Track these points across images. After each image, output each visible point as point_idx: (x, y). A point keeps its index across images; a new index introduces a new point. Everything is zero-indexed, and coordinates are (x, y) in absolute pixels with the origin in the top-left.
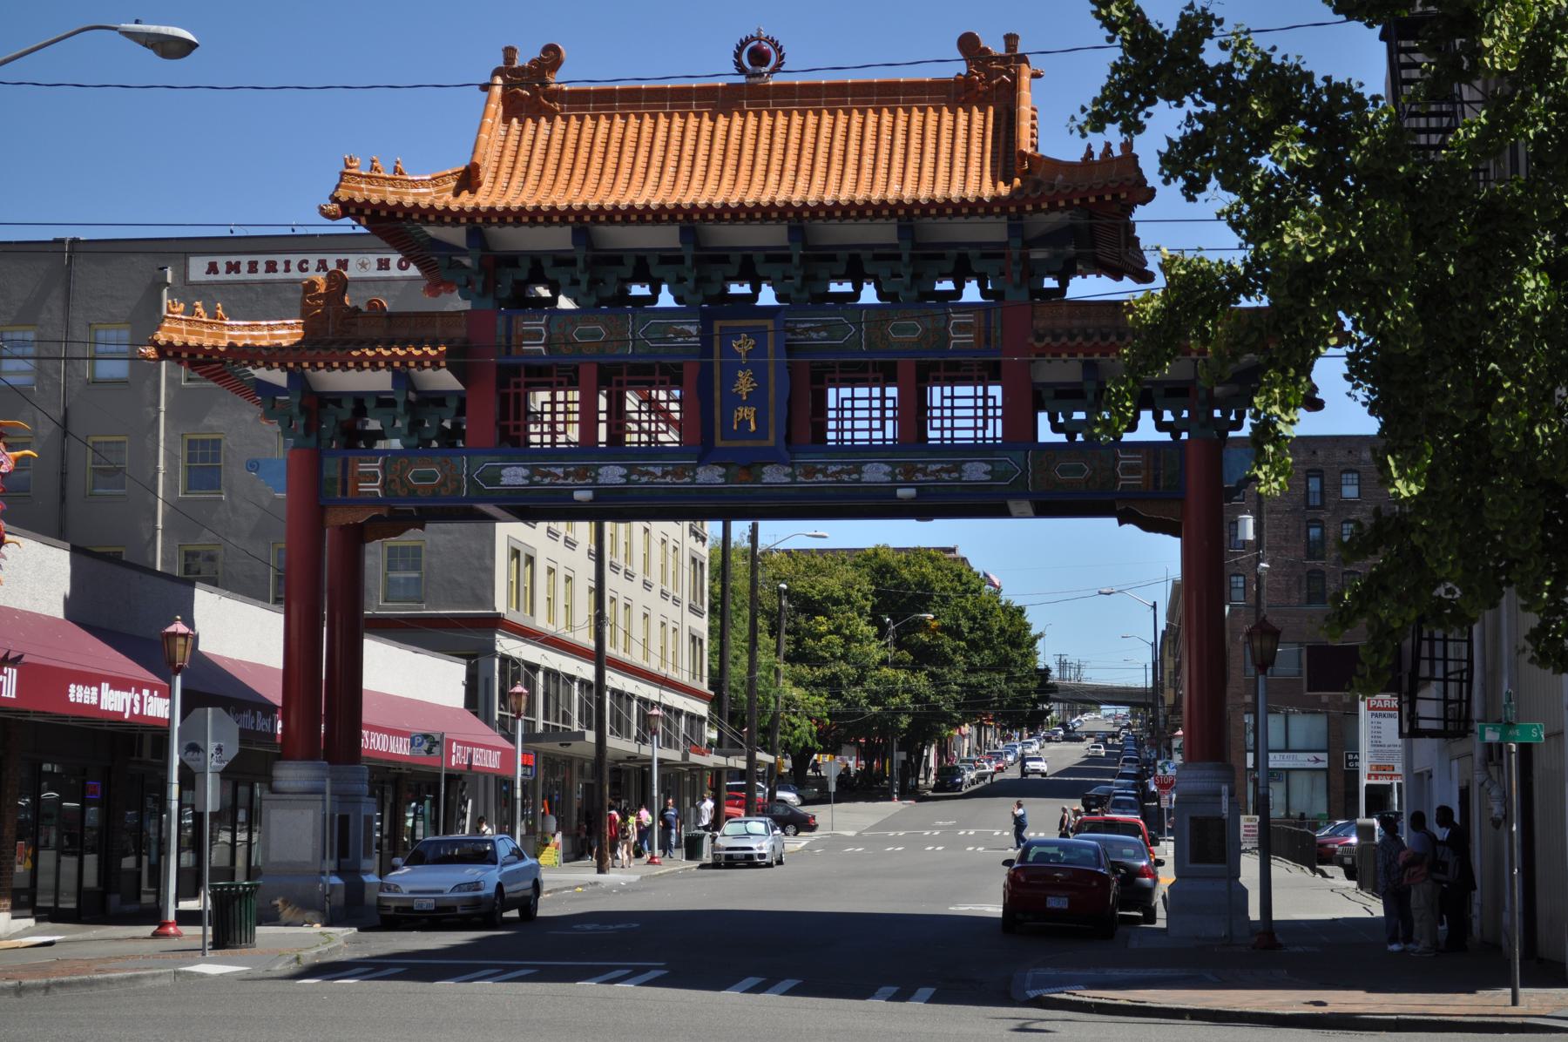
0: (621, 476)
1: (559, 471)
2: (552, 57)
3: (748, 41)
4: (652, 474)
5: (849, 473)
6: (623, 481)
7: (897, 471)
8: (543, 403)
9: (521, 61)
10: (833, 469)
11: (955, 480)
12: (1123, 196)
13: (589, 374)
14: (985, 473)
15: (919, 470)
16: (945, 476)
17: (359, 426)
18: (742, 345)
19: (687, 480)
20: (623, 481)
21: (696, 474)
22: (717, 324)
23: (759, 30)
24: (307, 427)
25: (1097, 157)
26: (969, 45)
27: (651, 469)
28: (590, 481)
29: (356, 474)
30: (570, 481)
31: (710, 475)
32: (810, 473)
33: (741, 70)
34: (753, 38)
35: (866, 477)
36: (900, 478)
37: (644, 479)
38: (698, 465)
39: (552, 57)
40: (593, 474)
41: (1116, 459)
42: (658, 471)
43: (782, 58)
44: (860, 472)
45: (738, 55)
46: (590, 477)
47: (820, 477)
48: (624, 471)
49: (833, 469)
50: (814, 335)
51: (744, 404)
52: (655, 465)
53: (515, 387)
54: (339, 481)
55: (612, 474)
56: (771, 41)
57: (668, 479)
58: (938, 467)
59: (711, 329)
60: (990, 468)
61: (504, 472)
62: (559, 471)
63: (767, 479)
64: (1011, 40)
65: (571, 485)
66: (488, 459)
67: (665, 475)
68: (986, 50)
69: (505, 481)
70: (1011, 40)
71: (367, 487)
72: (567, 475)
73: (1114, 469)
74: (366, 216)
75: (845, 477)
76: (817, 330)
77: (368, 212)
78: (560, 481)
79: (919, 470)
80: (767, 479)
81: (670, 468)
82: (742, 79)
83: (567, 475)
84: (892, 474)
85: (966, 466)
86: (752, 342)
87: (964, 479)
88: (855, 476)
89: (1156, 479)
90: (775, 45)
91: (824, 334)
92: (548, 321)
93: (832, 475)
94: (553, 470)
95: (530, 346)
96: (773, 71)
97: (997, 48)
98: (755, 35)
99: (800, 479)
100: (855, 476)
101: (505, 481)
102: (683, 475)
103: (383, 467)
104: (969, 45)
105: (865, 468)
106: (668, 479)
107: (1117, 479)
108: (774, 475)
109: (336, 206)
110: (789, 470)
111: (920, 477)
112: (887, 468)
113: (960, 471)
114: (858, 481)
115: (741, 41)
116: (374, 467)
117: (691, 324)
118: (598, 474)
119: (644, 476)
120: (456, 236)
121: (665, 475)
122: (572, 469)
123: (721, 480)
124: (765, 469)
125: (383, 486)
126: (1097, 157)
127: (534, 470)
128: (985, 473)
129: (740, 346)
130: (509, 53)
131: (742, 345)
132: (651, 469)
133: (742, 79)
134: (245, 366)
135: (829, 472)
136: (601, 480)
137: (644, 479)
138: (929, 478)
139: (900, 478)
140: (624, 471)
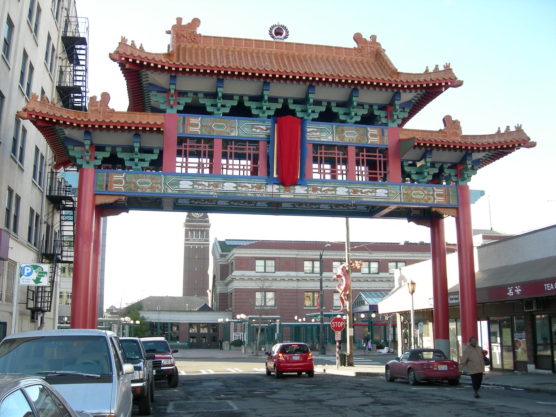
0: (233, 187)
1: (206, 184)
2: (196, 22)
4: (247, 187)
5: (331, 191)
6: (235, 189)
7: (350, 191)
9: (184, 23)
10: (324, 189)
14: (386, 194)
16: (370, 194)
19: (263, 190)
20: (235, 189)
21: (266, 188)
23: (278, 22)
26: (358, 38)
28: (220, 188)
30: (211, 188)
32: (315, 190)
33: (273, 37)
35: (338, 193)
36: (351, 194)
38: (267, 184)
39: (196, 22)
40: (221, 186)
43: (288, 32)
46: (220, 187)
47: (319, 192)
48: (235, 185)
49: (324, 189)
53: (185, 147)
58: (367, 190)
60: (387, 192)
61: (181, 182)
62: (206, 184)
63: (297, 191)
65: (211, 190)
66: (173, 177)
67: (253, 187)
68: (365, 39)
69: (181, 186)
71: (116, 187)
72: (209, 186)
76: (316, 132)
77: (130, 60)
78: (206, 188)
80: (297, 191)
81: (255, 185)
82: (272, 39)
83: (209, 186)
84: (348, 192)
85: (377, 191)
87: (377, 196)
91: (318, 134)
92: (201, 122)
93: (324, 191)
94: (203, 183)
95: (192, 129)
96: (285, 38)
98: (277, 25)
100: (333, 192)
101: (181, 186)
102: (260, 188)
103: (125, 178)
104: (358, 38)
105: (337, 189)
106: (254, 189)
107: (434, 199)
110: (306, 188)
111: (360, 194)
112: (347, 190)
113: (376, 193)
115: (272, 26)
117: (263, 125)
118: (223, 186)
119: (242, 187)
120: (161, 80)
121: (253, 187)
122: (212, 183)
123: (278, 191)
125: (124, 187)
127: (195, 183)
128: (386, 194)
130: (179, 20)
132: (247, 185)
133: (272, 39)
135: (323, 190)
136: (225, 189)
137: (244, 189)
138: (364, 195)
139: (351, 194)
140: (235, 185)
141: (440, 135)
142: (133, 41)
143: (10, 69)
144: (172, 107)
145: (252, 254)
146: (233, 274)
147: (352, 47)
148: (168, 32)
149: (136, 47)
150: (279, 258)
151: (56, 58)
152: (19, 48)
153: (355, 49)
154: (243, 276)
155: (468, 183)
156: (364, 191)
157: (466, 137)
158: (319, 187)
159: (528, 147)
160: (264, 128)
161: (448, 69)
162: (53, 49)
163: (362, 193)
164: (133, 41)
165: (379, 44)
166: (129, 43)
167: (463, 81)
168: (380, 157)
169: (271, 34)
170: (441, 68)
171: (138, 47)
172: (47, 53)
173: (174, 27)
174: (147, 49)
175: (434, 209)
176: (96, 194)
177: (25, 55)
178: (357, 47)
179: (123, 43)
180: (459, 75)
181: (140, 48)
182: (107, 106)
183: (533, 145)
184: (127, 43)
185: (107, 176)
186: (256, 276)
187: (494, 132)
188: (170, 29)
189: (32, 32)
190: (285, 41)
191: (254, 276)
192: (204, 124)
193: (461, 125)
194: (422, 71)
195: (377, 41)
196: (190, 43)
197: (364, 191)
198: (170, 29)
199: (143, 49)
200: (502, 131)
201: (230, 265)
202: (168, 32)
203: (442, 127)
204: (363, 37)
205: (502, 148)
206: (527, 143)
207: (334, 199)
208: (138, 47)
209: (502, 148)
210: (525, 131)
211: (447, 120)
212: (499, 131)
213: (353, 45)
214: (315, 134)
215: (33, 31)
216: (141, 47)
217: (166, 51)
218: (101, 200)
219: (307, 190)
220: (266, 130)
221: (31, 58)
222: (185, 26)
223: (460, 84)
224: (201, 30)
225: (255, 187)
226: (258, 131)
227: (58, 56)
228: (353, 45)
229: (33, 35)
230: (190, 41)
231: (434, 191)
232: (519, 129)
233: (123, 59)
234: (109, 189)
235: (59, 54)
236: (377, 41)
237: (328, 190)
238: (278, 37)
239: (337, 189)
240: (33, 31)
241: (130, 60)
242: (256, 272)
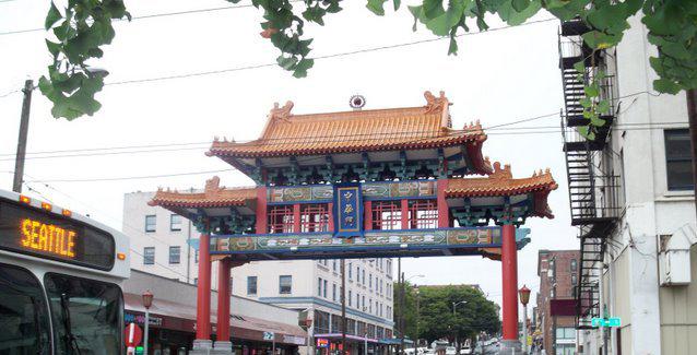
13: (297, 209)
18: (348, 195)
31: (337, 242)
108: (359, 241)
131: (348, 195)
179: (216, 142)
232: (548, 171)
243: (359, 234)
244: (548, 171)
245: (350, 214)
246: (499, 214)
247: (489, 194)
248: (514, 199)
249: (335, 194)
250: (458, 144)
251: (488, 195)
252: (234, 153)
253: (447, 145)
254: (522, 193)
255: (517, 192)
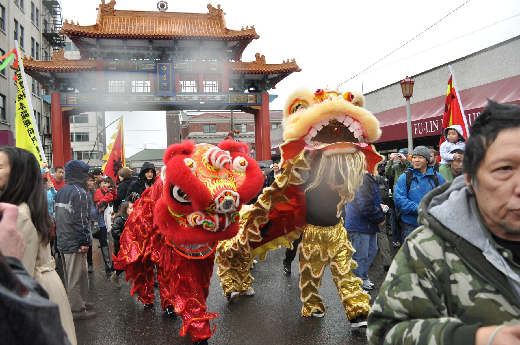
3: (158, 3)
4: (144, 98)
5: (189, 98)
8: (112, 84)
10: (185, 98)
11: (213, 100)
12: (252, 37)
15: (205, 98)
16: (211, 99)
17: (67, 89)
21: (154, 98)
22: (158, 64)
24: (56, 86)
25: (245, 29)
26: (209, 6)
27: (143, 97)
29: (70, 99)
31: (158, 99)
33: (159, 9)
34: (161, 2)
35: (193, 100)
36: (201, 100)
37: (142, 100)
39: (113, 3)
41: (248, 96)
42: (145, 98)
44: (192, 98)
45: (157, 6)
47: (183, 100)
48: (137, 98)
49: (185, 98)
50: (180, 67)
51: (165, 82)
52: (144, 96)
54: (65, 100)
55: (134, 99)
56: (165, 2)
57: (147, 100)
58: (209, 97)
59: (157, 65)
64: (219, 6)
67: (147, 98)
70: (219, 6)
73: (247, 99)
74: (71, 34)
75: (189, 99)
76: (181, 66)
77: (71, 33)
79: (205, 98)
82: (159, 11)
85: (216, 97)
86: (166, 68)
88: (191, 99)
89: (256, 101)
90: (166, 3)
92: (116, 63)
96: (166, 9)
97: (216, 7)
99: (178, 100)
100: (191, 99)
103: (76, 97)
104: (209, 6)
105: (193, 97)
106: (147, 100)
107: (248, 100)
108: (172, 99)
109: (63, 31)
110: (176, 98)
111: (205, 99)
113: (214, 98)
114: (191, 100)
116: (74, 96)
119: (141, 99)
124: (170, 97)
126: (245, 29)
129: (163, 69)
132: (143, 97)
133: (159, 11)
134: (40, 71)
137: (142, 100)
139: (201, 100)
140: (137, 98)
141: (252, 64)
142: (72, 21)
143: (6, 35)
144: (99, 56)
145: (201, 121)
146: (190, 134)
147: (206, 13)
148: (97, 9)
149: (74, 24)
150: (218, 123)
151: (40, 15)
152: (10, 21)
153: (208, 14)
154: (195, 135)
155: (268, 91)
156: (208, 98)
157: (268, 65)
158: (183, 97)
159: (298, 71)
160: (151, 65)
161: (253, 29)
162: (37, 10)
163: (207, 99)
164: (72, 21)
165: (222, 10)
166: (70, 22)
167: (259, 36)
168: (218, 78)
169: (158, 7)
170: (250, 28)
171: (76, 24)
172: (32, 14)
173: (100, 5)
174: (81, 25)
175: (248, 106)
176: (61, 106)
177: (16, 22)
178: (209, 12)
180: (258, 32)
181: (77, 24)
182: (63, 57)
183: (300, 70)
184: (69, 23)
185: (67, 95)
186: (204, 136)
187: (281, 62)
188: (98, 7)
189: (18, 7)
190: (166, 11)
191: (203, 136)
192: (118, 65)
193: (266, 58)
194: (240, 29)
195: (221, 8)
196: (110, 15)
197: (208, 98)
198: (98, 7)
199: (79, 25)
200: (285, 62)
201: (188, 128)
202: (97, 9)
203: (254, 59)
204: (213, 6)
205: (286, 71)
206: (297, 69)
207: (192, 103)
208: (76, 24)
209: (286, 71)
210: (297, 63)
211: (257, 55)
212: (284, 62)
213: (207, 11)
214: (180, 67)
215: (20, 6)
216: (78, 24)
217: (94, 23)
218: (64, 109)
219: (176, 99)
220: (153, 67)
221: (20, 22)
222: (107, 5)
223: (258, 37)
224: (116, 7)
225: (147, 98)
226: (148, 67)
227: (41, 14)
228: (207, 11)
229: (20, 9)
230: (110, 14)
231: (248, 96)
233: (67, 32)
234: (68, 103)
235: (41, 12)
236: (221, 8)
237: (188, 98)
238: (162, 9)
239: (193, 97)
240: (20, 6)
241: (71, 33)
242: (204, 133)
243: (172, 95)
244: (293, 61)
245: (165, 82)
246: (259, 85)
247: (255, 73)
248: (271, 76)
249: (156, 66)
250: (237, 40)
251: (255, 73)
252: (82, 34)
253: (230, 40)
254: (276, 73)
255: (272, 73)
